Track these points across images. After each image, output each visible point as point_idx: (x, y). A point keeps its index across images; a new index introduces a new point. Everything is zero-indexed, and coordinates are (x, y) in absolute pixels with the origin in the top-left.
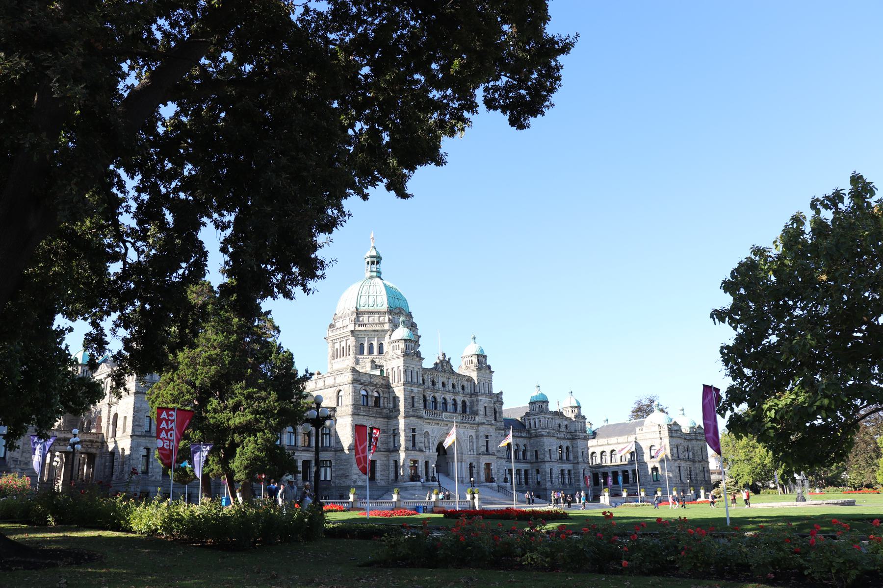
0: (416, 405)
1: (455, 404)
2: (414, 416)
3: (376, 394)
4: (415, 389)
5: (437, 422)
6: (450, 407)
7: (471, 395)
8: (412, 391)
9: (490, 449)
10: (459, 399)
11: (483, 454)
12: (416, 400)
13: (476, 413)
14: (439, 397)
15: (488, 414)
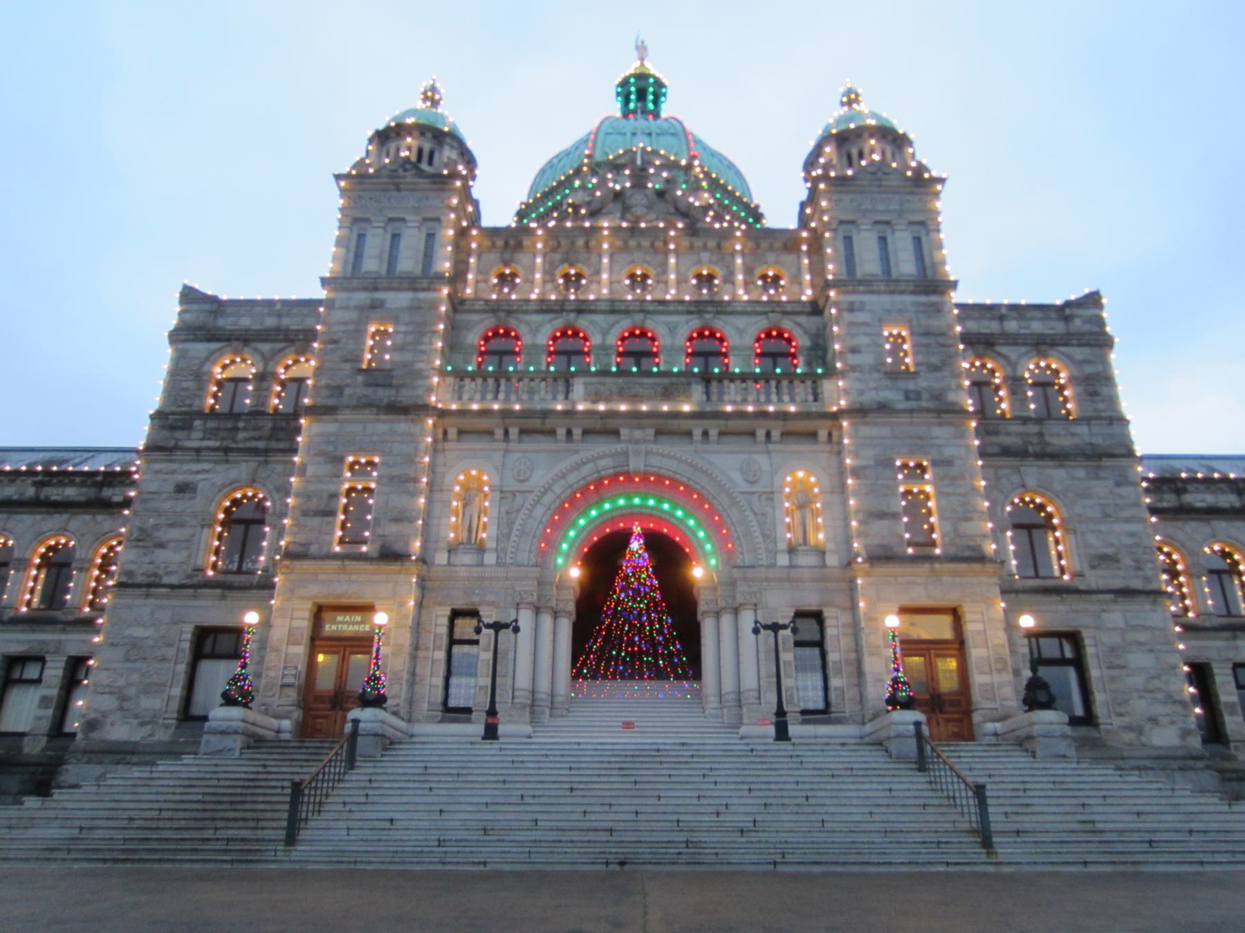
4: (399, 300)
5: (536, 426)
11: (882, 557)
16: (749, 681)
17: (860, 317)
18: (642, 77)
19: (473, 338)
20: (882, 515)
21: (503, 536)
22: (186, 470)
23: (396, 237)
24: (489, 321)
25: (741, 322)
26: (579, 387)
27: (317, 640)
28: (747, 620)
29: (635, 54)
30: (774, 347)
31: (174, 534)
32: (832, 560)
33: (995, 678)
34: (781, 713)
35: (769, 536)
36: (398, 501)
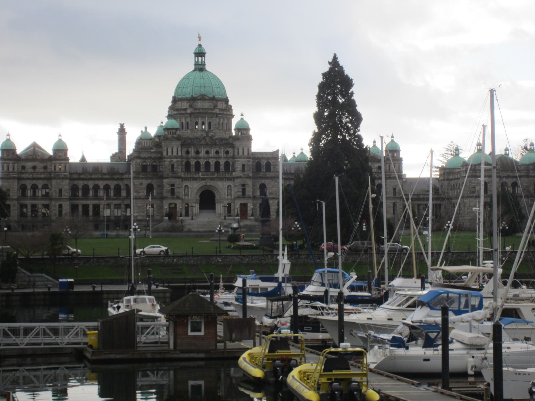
0: (175, 169)
1: (217, 164)
2: (172, 177)
3: (154, 164)
4: (174, 160)
5: (195, 179)
6: (212, 169)
7: (233, 157)
8: (172, 161)
9: (246, 193)
10: (222, 162)
11: (238, 197)
12: (175, 166)
13: (234, 171)
14: (202, 162)
15: (246, 169)
16: (222, 212)
17: (239, 163)
18: (201, 53)
19: (184, 163)
20: (239, 192)
21: (191, 194)
22: (141, 181)
23: (172, 149)
24: (185, 160)
25: (222, 160)
26: (200, 174)
27: (170, 208)
28: (222, 205)
29: (198, 39)
30: (227, 164)
31: (141, 191)
32: (233, 197)
33: (249, 212)
34: (225, 217)
35: (225, 194)
36: (178, 190)
